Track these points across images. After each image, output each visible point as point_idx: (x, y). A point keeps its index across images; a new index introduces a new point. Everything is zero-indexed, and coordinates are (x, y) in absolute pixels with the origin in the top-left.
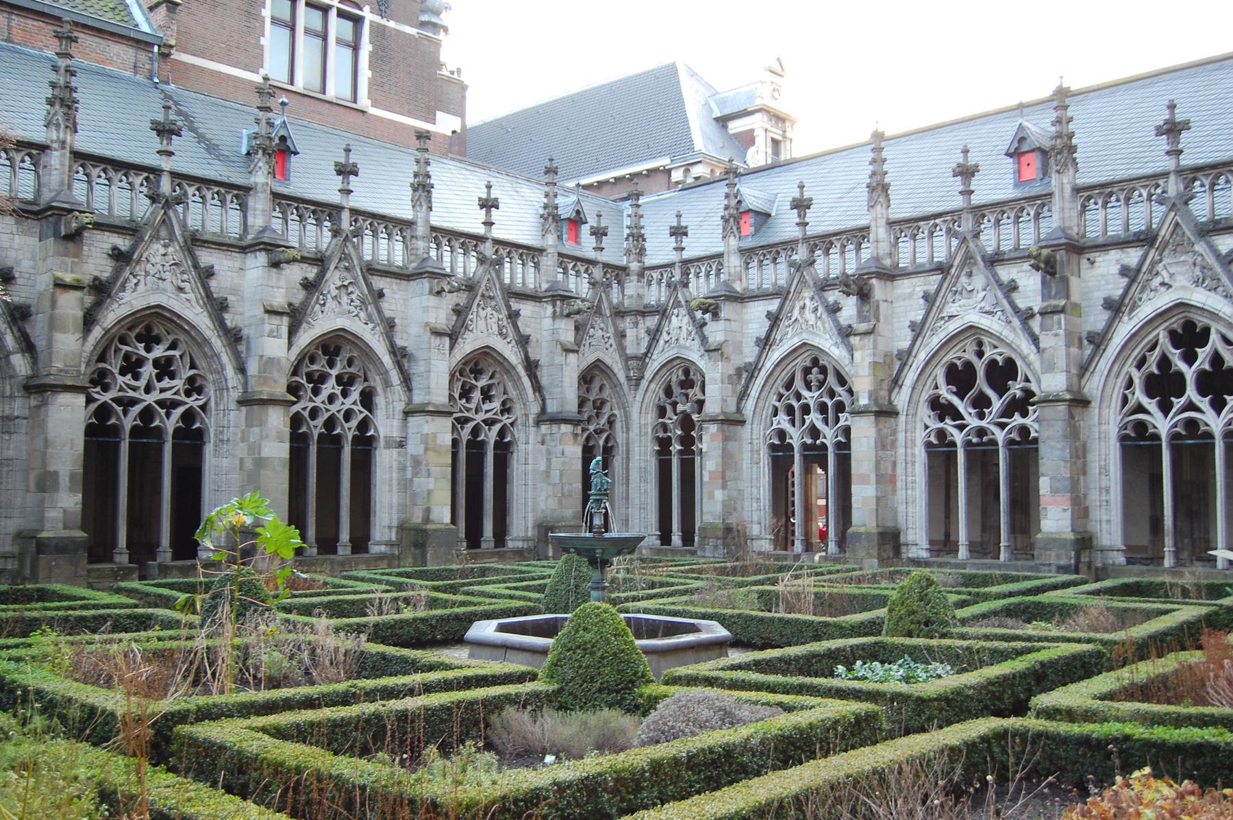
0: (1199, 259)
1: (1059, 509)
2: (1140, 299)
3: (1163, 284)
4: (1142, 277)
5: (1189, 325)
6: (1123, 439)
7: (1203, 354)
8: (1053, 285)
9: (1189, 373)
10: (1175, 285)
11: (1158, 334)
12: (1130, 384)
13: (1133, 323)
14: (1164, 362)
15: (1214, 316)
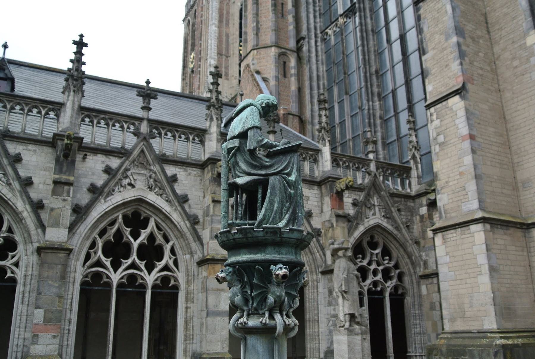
0: (154, 175)
1: (49, 336)
2: (113, 191)
3: (130, 184)
4: (119, 176)
5: (136, 214)
6: (84, 284)
7: (144, 235)
8: (65, 164)
9: (135, 244)
10: (137, 187)
11: (118, 216)
12: (93, 245)
13: (107, 205)
14: (119, 234)
15: (158, 210)
